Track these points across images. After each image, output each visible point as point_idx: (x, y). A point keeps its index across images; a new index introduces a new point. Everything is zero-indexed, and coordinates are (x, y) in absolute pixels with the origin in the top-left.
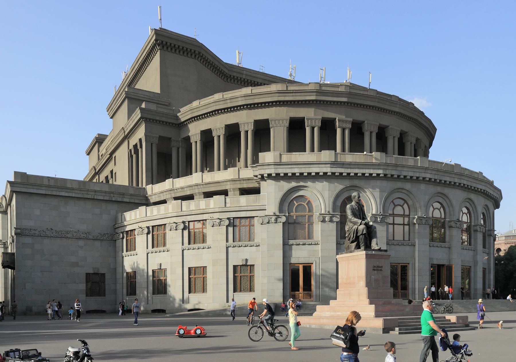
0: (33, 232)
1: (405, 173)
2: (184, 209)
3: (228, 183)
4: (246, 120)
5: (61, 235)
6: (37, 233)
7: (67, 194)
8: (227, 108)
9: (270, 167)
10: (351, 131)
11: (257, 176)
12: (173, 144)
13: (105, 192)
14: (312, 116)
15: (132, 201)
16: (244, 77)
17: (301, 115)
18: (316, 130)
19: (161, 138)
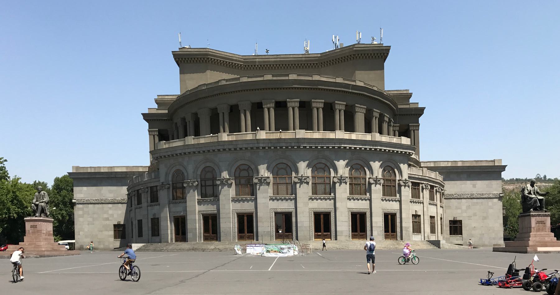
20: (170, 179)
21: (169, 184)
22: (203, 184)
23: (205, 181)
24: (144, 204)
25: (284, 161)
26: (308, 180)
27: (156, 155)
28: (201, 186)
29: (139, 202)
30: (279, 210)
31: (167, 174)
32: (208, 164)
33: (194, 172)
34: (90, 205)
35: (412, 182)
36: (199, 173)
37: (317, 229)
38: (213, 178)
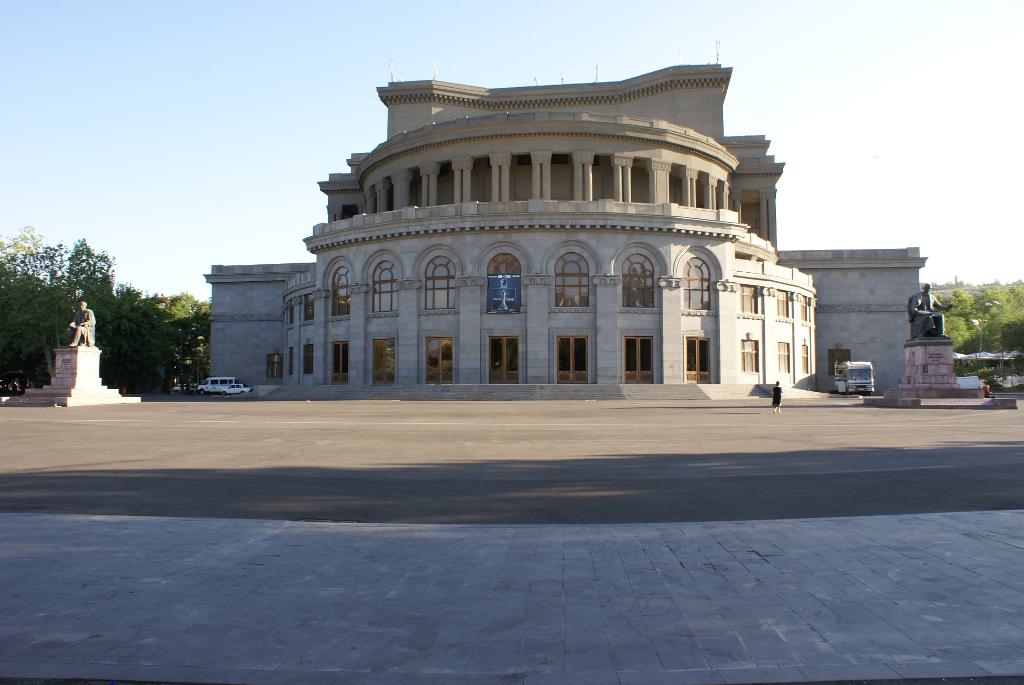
5: (247, 319)
20: (330, 282)
21: (328, 291)
22: (377, 287)
24: (296, 322)
25: (508, 250)
26: (548, 281)
27: (311, 246)
28: (375, 291)
29: (292, 321)
30: (497, 334)
31: (325, 275)
32: (385, 257)
33: (363, 271)
35: (742, 285)
36: (371, 272)
37: (563, 364)
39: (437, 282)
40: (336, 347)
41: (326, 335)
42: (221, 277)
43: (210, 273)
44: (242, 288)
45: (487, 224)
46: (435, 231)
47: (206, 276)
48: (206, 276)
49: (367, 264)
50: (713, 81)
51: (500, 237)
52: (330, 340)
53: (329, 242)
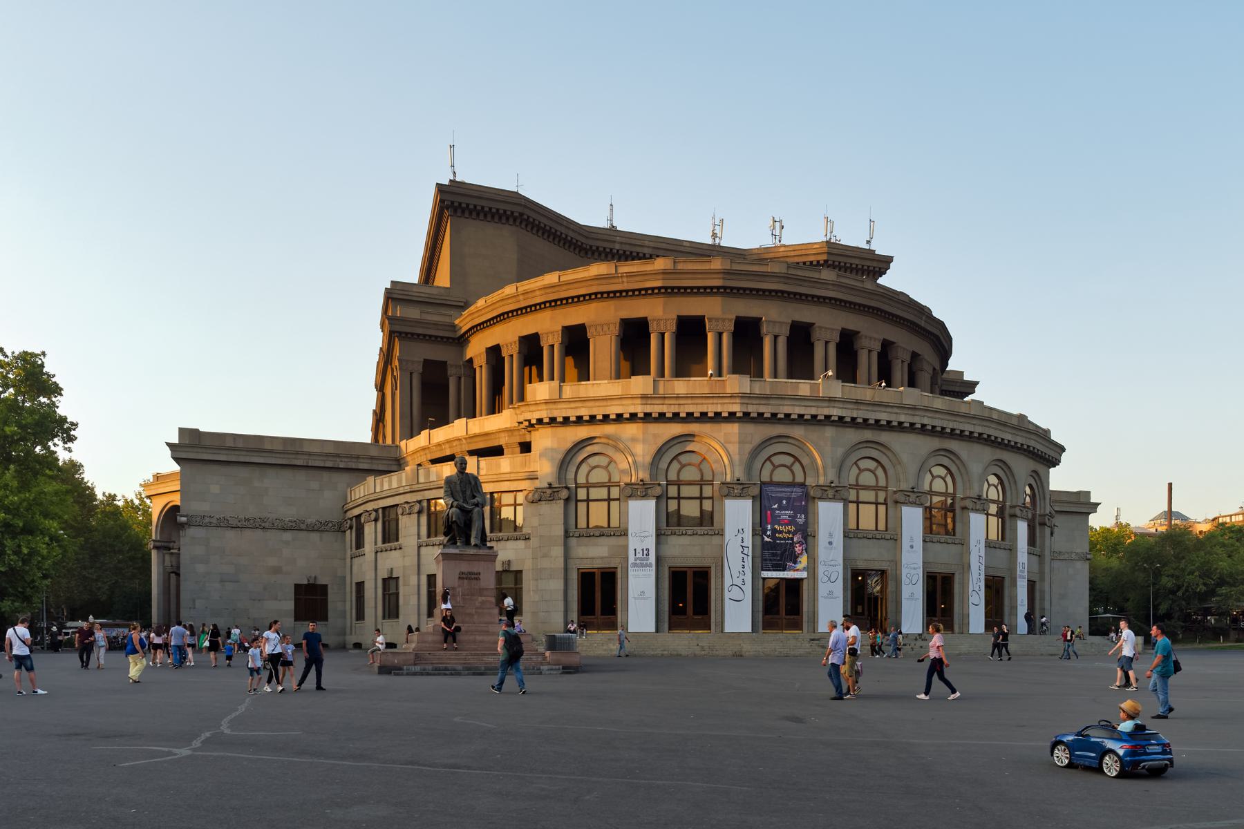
0: (207, 520)
1: (787, 410)
2: (422, 480)
3: (502, 435)
4: (549, 326)
6: (214, 521)
7: (261, 460)
8: (521, 309)
9: (540, 407)
10: (790, 340)
11: (520, 423)
12: (451, 371)
13: (327, 455)
14: (719, 314)
15: (375, 467)
16: (617, 246)
17: (639, 314)
18: (726, 339)
19: (427, 363)
22: (673, 491)
23: (679, 486)
34: (230, 534)
38: (702, 480)
39: (862, 493)
40: (587, 578)
41: (567, 557)
42: (194, 449)
43: (176, 440)
44: (243, 472)
45: (860, 414)
46: (788, 416)
47: (168, 444)
48: (168, 444)
49: (660, 453)
50: (884, 263)
51: (868, 435)
52: (574, 565)
53: (585, 413)
